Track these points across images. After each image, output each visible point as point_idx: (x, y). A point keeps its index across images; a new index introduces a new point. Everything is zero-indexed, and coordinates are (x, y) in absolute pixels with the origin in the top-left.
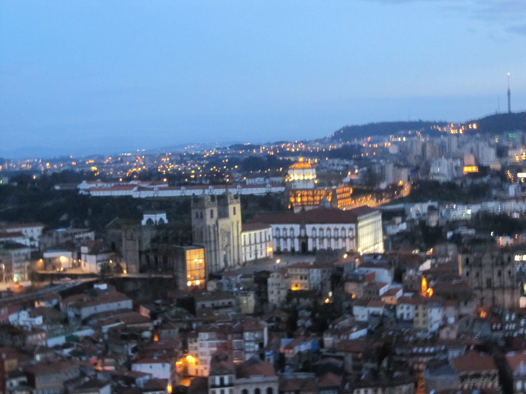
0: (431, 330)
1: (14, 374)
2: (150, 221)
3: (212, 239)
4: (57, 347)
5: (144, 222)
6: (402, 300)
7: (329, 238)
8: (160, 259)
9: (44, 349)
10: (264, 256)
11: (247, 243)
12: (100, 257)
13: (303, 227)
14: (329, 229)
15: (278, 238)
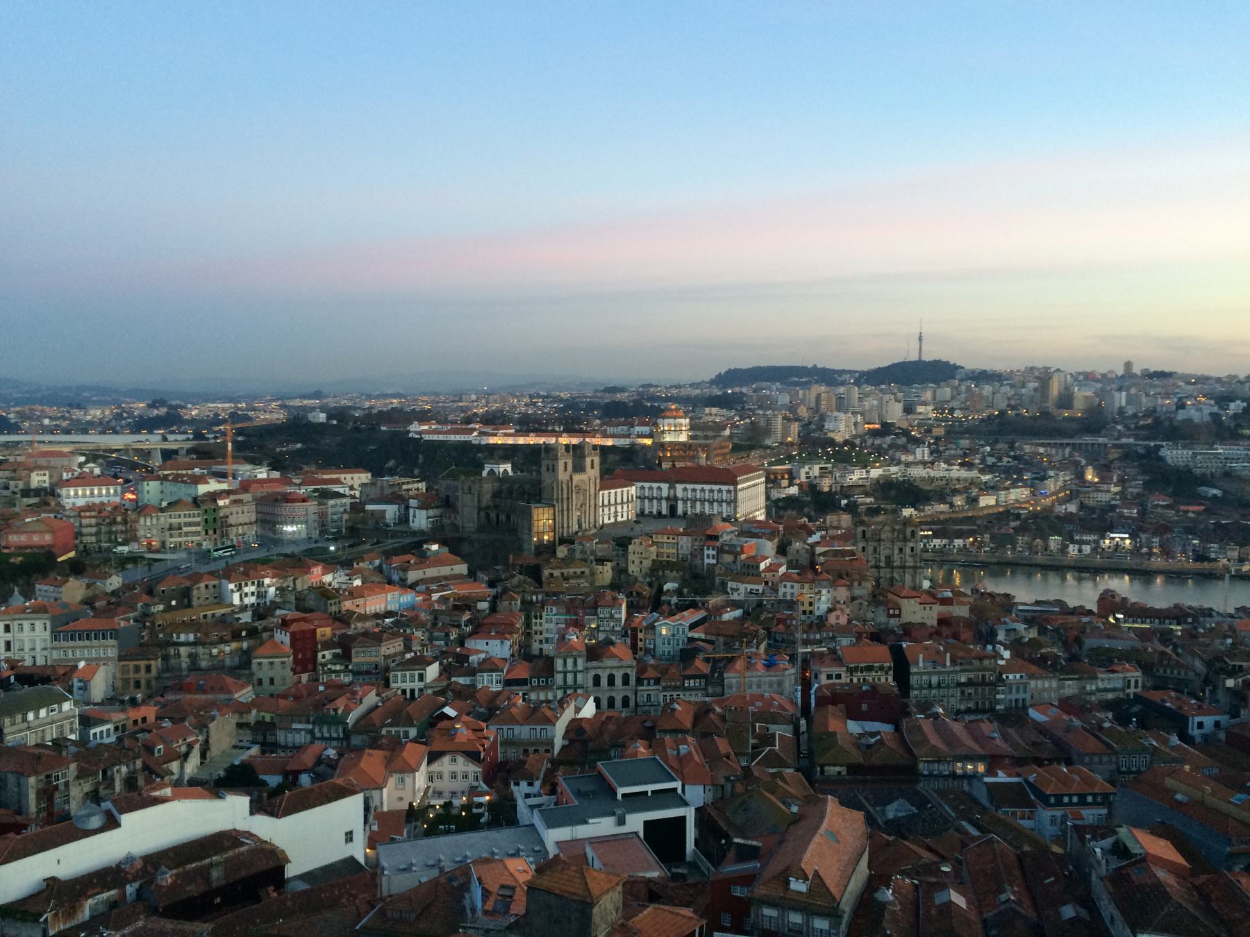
0: (817, 613)
1: (328, 645)
2: (492, 472)
3: (565, 496)
4: (377, 616)
5: (484, 474)
6: (785, 577)
7: (702, 501)
8: (503, 517)
9: (363, 618)
10: (625, 518)
11: (606, 502)
12: (431, 512)
13: (672, 487)
14: (703, 490)
15: (641, 498)
